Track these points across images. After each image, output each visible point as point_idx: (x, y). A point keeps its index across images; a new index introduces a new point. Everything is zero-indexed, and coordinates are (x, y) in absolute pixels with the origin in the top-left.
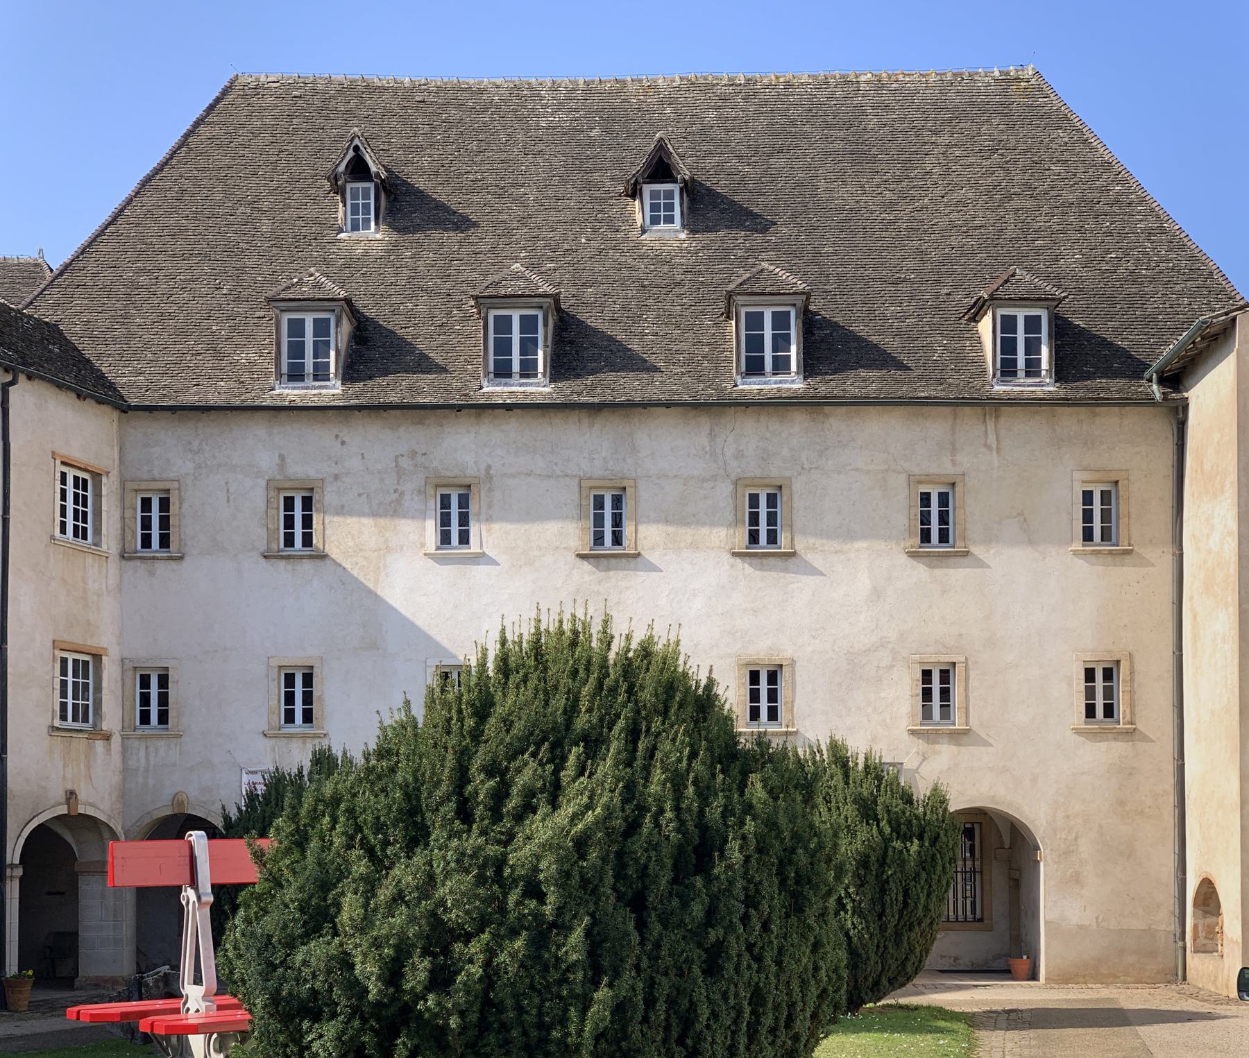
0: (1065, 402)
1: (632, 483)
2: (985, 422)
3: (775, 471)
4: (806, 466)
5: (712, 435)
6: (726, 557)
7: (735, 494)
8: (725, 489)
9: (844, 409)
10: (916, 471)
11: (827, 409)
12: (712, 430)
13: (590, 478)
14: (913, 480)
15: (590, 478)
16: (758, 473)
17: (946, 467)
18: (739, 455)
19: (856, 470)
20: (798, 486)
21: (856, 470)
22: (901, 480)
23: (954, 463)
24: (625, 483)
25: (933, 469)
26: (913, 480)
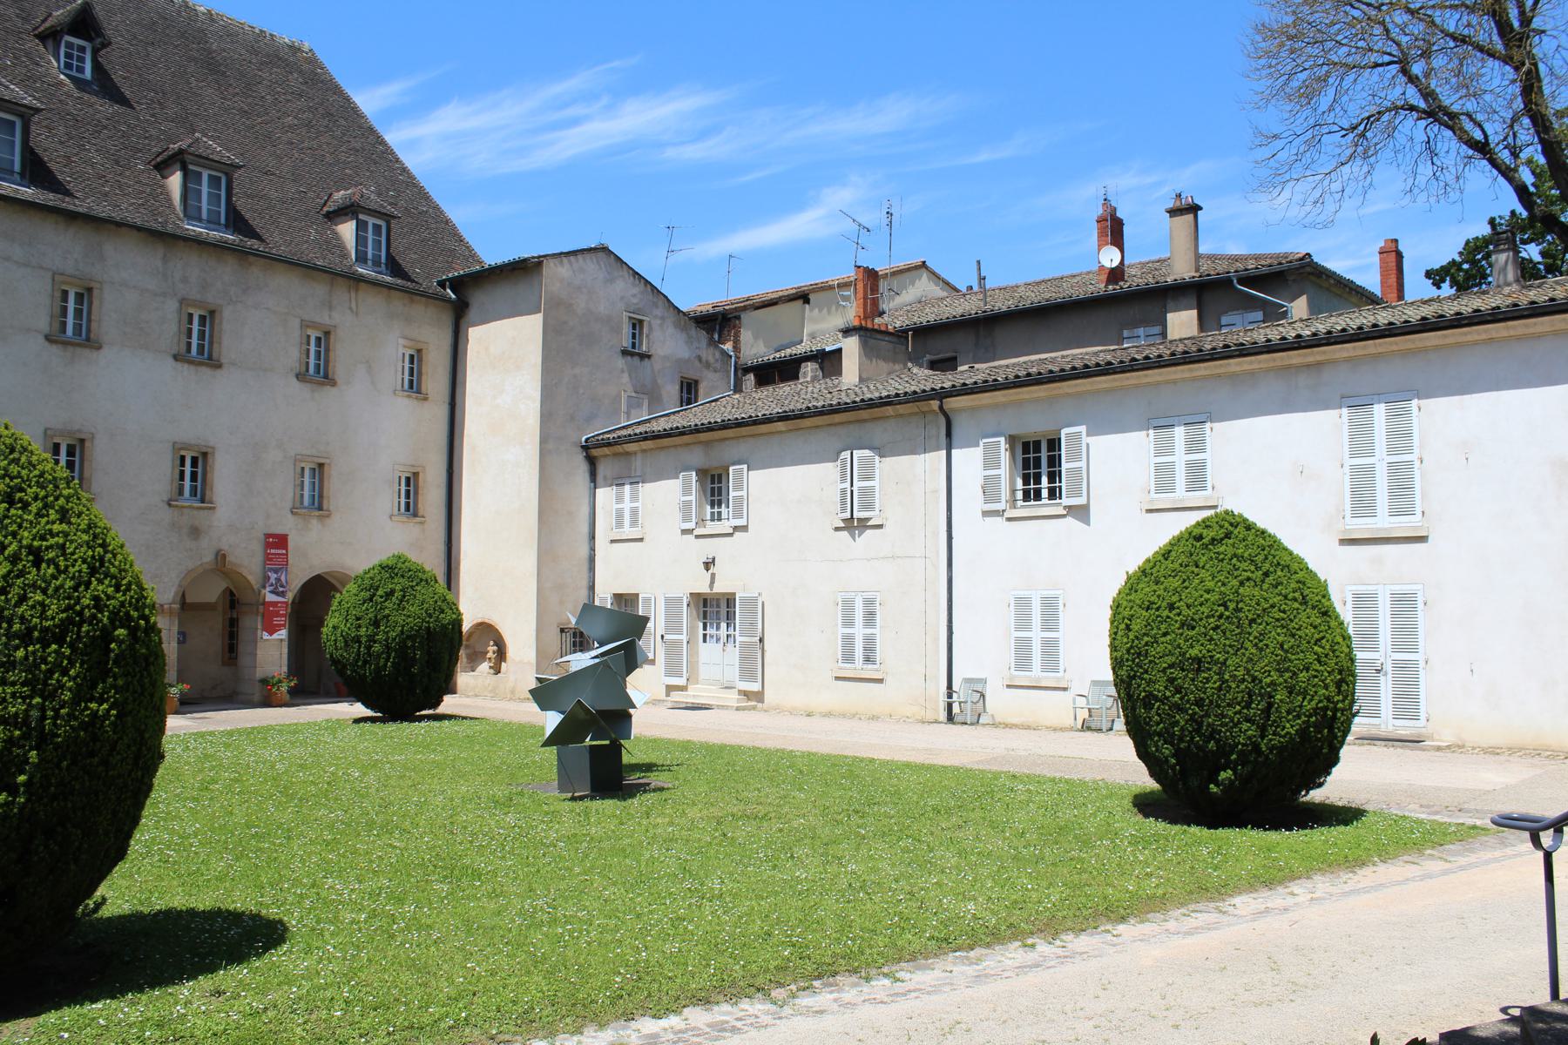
0: (389, 287)
1: (98, 285)
2: (350, 292)
3: (212, 298)
4: (234, 299)
5: (165, 260)
6: (171, 360)
7: (180, 310)
8: (172, 306)
9: (262, 261)
10: (306, 317)
11: (252, 259)
12: (165, 256)
13: (62, 274)
14: (305, 325)
15: (62, 274)
16: (198, 297)
17: (324, 318)
18: (185, 280)
19: (267, 309)
20: (227, 313)
21: (267, 309)
22: (297, 321)
23: (330, 316)
24: (93, 284)
25: (317, 319)
26: (305, 325)
